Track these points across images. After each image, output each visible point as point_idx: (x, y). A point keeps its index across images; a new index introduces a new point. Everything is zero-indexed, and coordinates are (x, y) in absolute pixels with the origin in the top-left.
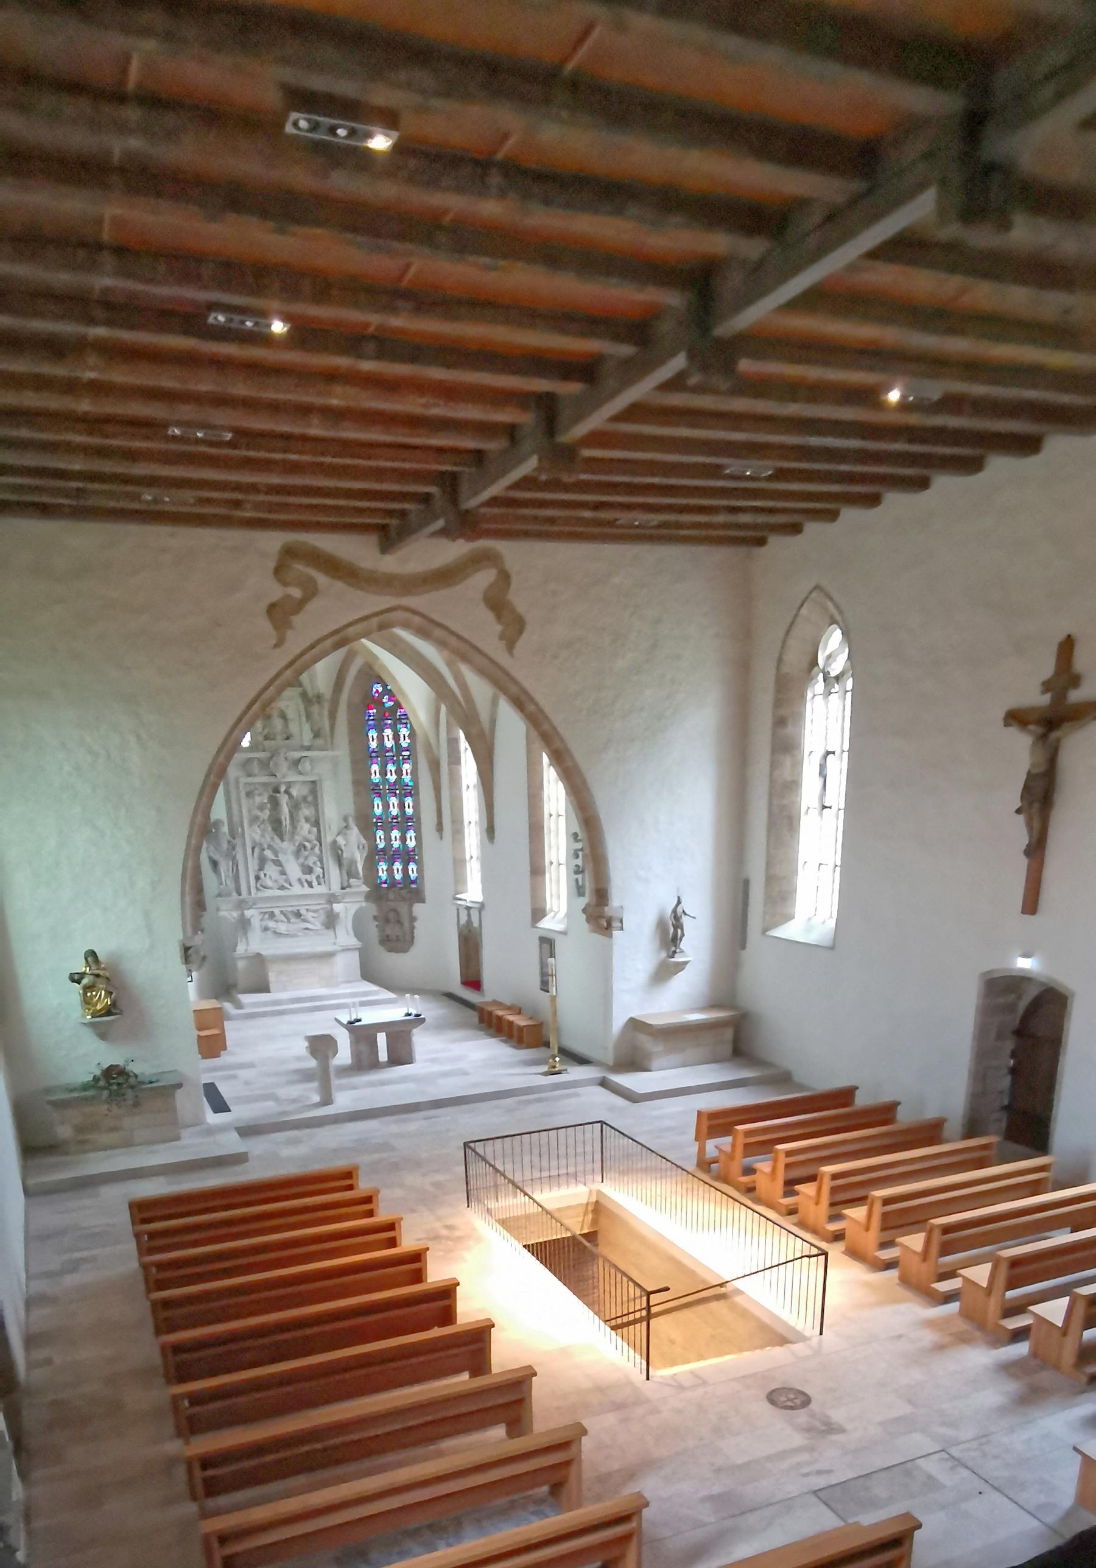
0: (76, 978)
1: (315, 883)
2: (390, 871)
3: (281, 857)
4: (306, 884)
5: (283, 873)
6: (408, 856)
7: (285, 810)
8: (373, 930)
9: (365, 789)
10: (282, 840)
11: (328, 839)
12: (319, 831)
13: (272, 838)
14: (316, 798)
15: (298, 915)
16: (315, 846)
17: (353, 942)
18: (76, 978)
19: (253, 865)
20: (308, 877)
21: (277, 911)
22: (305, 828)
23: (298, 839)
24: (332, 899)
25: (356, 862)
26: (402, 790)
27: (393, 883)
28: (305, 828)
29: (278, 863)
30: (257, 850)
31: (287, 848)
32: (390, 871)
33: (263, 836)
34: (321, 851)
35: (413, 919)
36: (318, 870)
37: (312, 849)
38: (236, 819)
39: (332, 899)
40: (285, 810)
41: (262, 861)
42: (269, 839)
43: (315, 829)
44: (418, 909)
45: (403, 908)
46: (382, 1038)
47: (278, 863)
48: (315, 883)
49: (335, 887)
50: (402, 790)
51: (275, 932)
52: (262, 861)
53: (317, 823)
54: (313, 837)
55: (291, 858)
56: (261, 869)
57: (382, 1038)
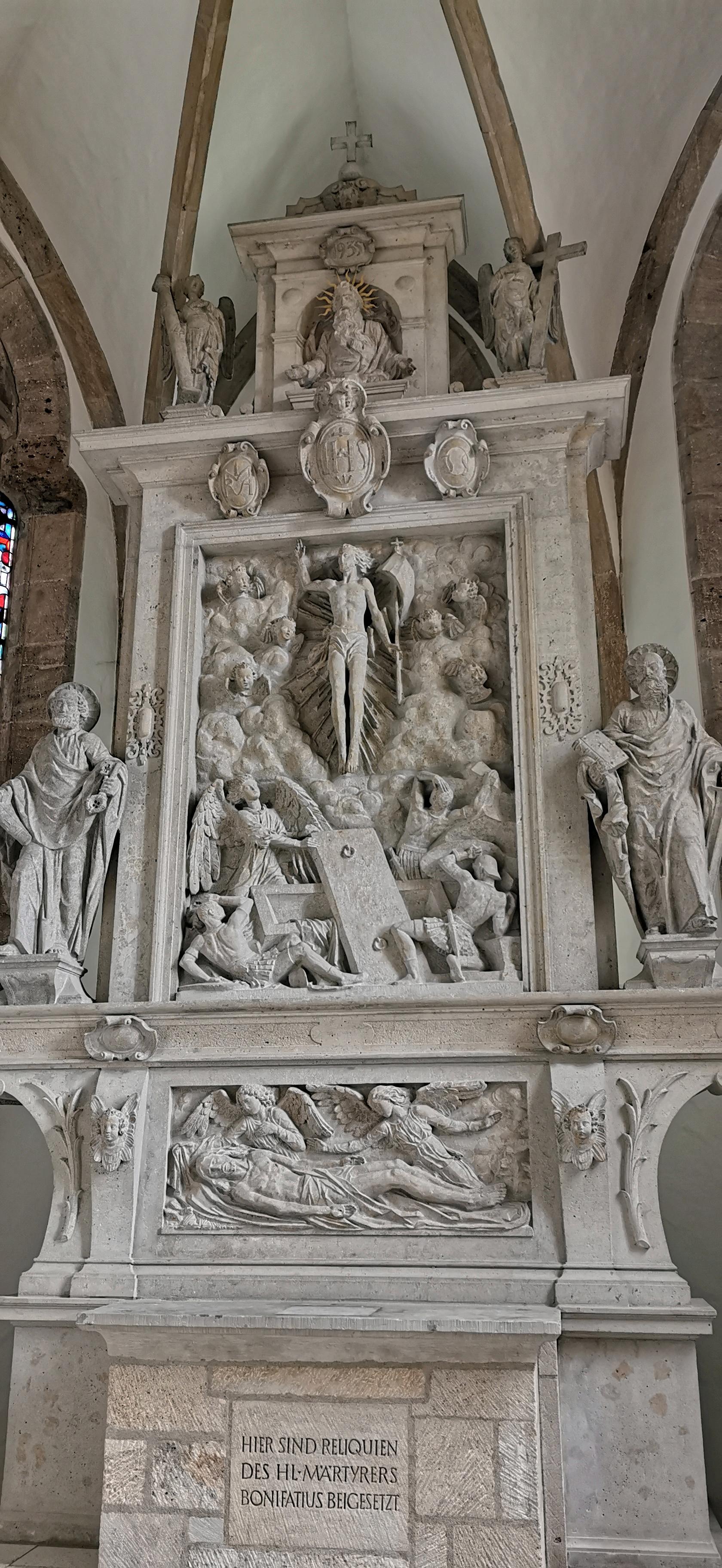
1: (464, 957)
3: (322, 842)
4: (417, 960)
5: (320, 910)
7: (353, 644)
10: (335, 771)
11: (538, 749)
12: (504, 730)
13: (291, 761)
14: (497, 600)
15: (362, 1110)
16: (481, 780)
17: (665, 1292)
19: (179, 865)
20: (435, 929)
21: (256, 1087)
22: (436, 716)
23: (405, 758)
25: (680, 841)
28: (436, 716)
29: (302, 866)
30: (212, 809)
33: (253, 751)
34: (509, 813)
36: (484, 897)
37: (459, 802)
38: (141, 680)
40: (353, 644)
42: (274, 761)
43: (484, 722)
47: (302, 866)
48: (464, 957)
49: (571, 972)
51: (231, 1198)
52: (232, 849)
54: (474, 754)
55: (368, 843)
56: (224, 885)
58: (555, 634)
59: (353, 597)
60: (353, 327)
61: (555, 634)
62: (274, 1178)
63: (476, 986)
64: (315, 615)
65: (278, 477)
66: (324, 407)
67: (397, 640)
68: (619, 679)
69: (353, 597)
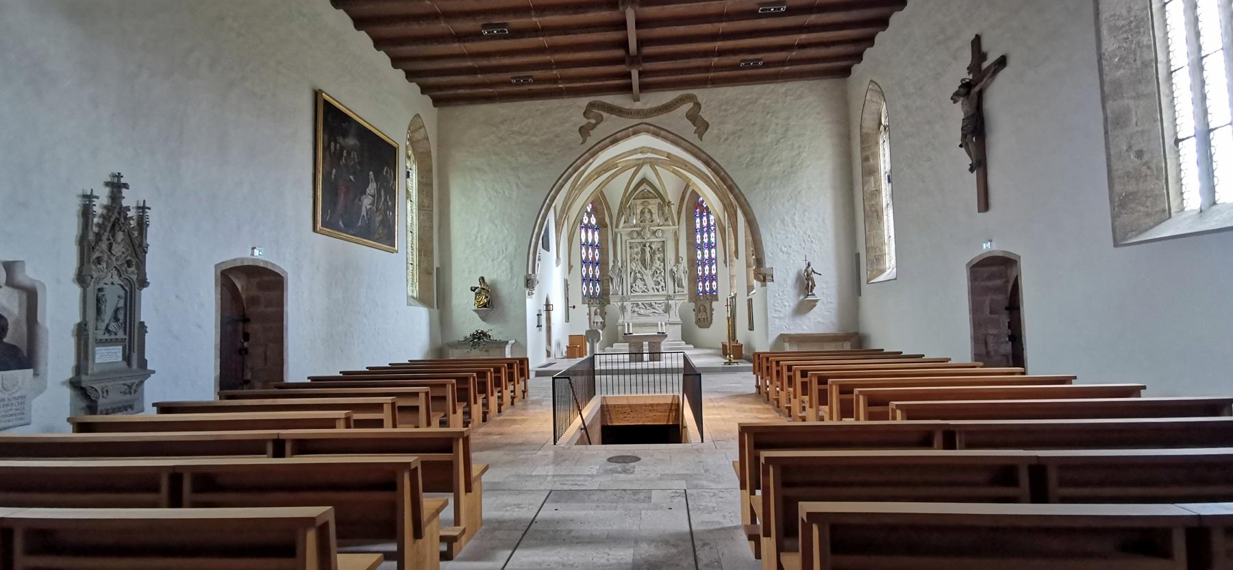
0: (473, 289)
2: (704, 287)
6: (712, 278)
7: (648, 256)
8: (692, 317)
9: (693, 246)
11: (668, 268)
18: (473, 289)
19: (630, 280)
22: (657, 264)
24: (669, 297)
26: (710, 246)
27: (704, 292)
28: (657, 264)
29: (643, 280)
31: (649, 272)
32: (704, 287)
35: (712, 310)
39: (669, 297)
41: (635, 279)
44: (714, 303)
45: (707, 305)
46: (646, 343)
47: (643, 280)
50: (710, 246)
52: (635, 279)
53: (664, 260)
57: (646, 343)
58: (670, 255)
59: (648, 249)
60: (647, 216)
61: (670, 255)
62: (642, 311)
63: (661, 292)
64: (643, 251)
65: (639, 234)
66: (644, 228)
67: (653, 253)
68: (677, 261)
69: (648, 249)
